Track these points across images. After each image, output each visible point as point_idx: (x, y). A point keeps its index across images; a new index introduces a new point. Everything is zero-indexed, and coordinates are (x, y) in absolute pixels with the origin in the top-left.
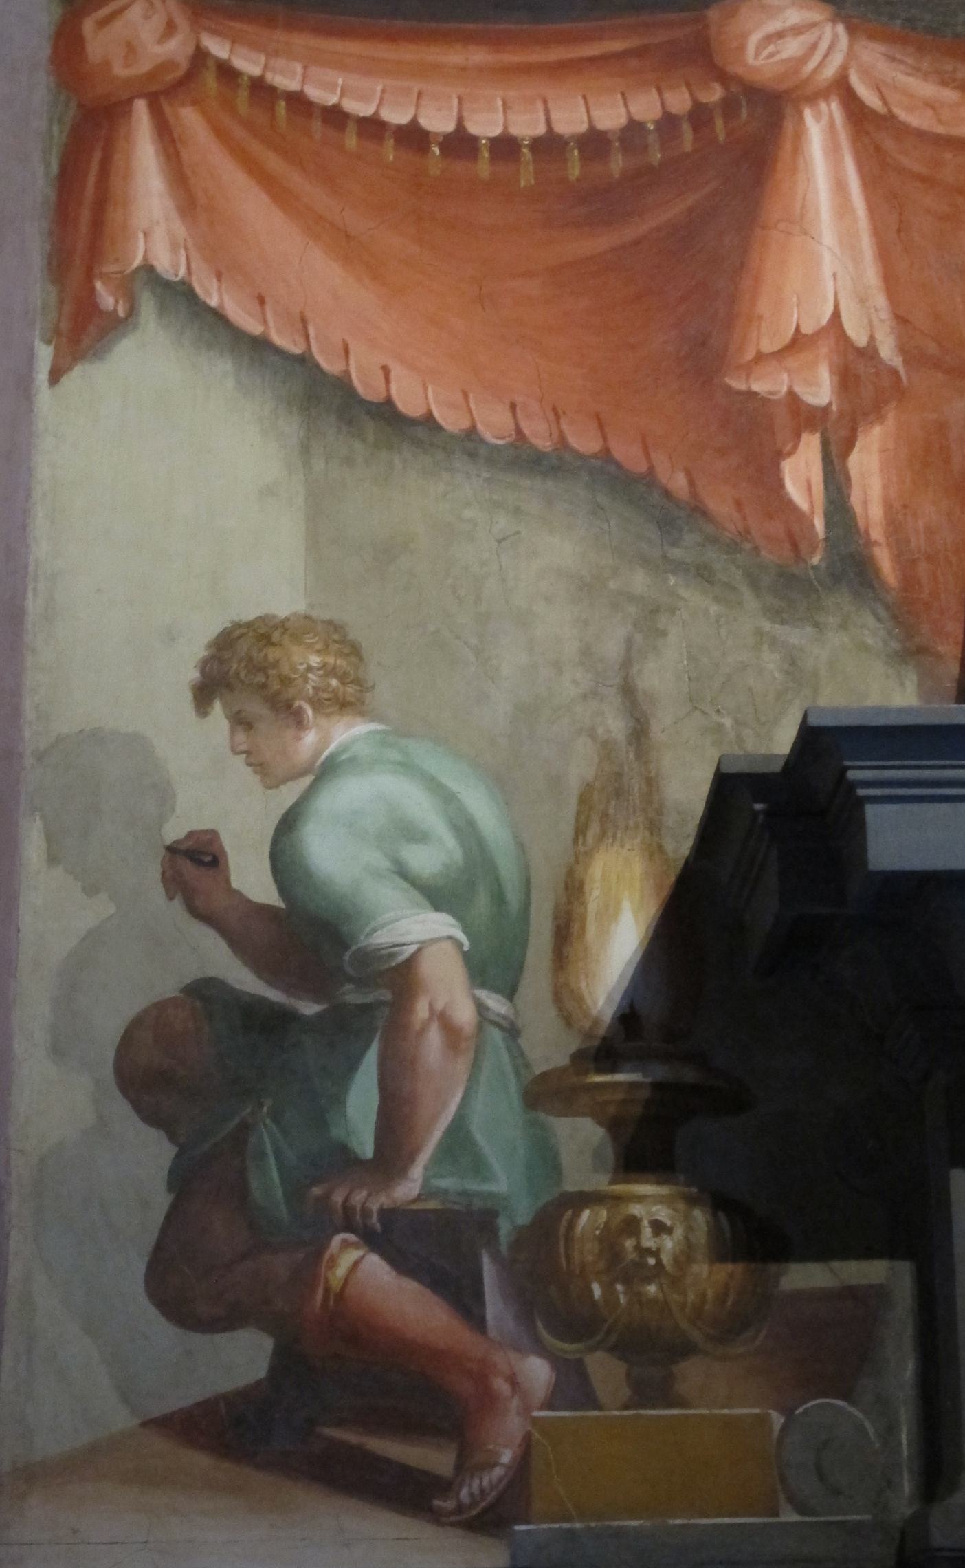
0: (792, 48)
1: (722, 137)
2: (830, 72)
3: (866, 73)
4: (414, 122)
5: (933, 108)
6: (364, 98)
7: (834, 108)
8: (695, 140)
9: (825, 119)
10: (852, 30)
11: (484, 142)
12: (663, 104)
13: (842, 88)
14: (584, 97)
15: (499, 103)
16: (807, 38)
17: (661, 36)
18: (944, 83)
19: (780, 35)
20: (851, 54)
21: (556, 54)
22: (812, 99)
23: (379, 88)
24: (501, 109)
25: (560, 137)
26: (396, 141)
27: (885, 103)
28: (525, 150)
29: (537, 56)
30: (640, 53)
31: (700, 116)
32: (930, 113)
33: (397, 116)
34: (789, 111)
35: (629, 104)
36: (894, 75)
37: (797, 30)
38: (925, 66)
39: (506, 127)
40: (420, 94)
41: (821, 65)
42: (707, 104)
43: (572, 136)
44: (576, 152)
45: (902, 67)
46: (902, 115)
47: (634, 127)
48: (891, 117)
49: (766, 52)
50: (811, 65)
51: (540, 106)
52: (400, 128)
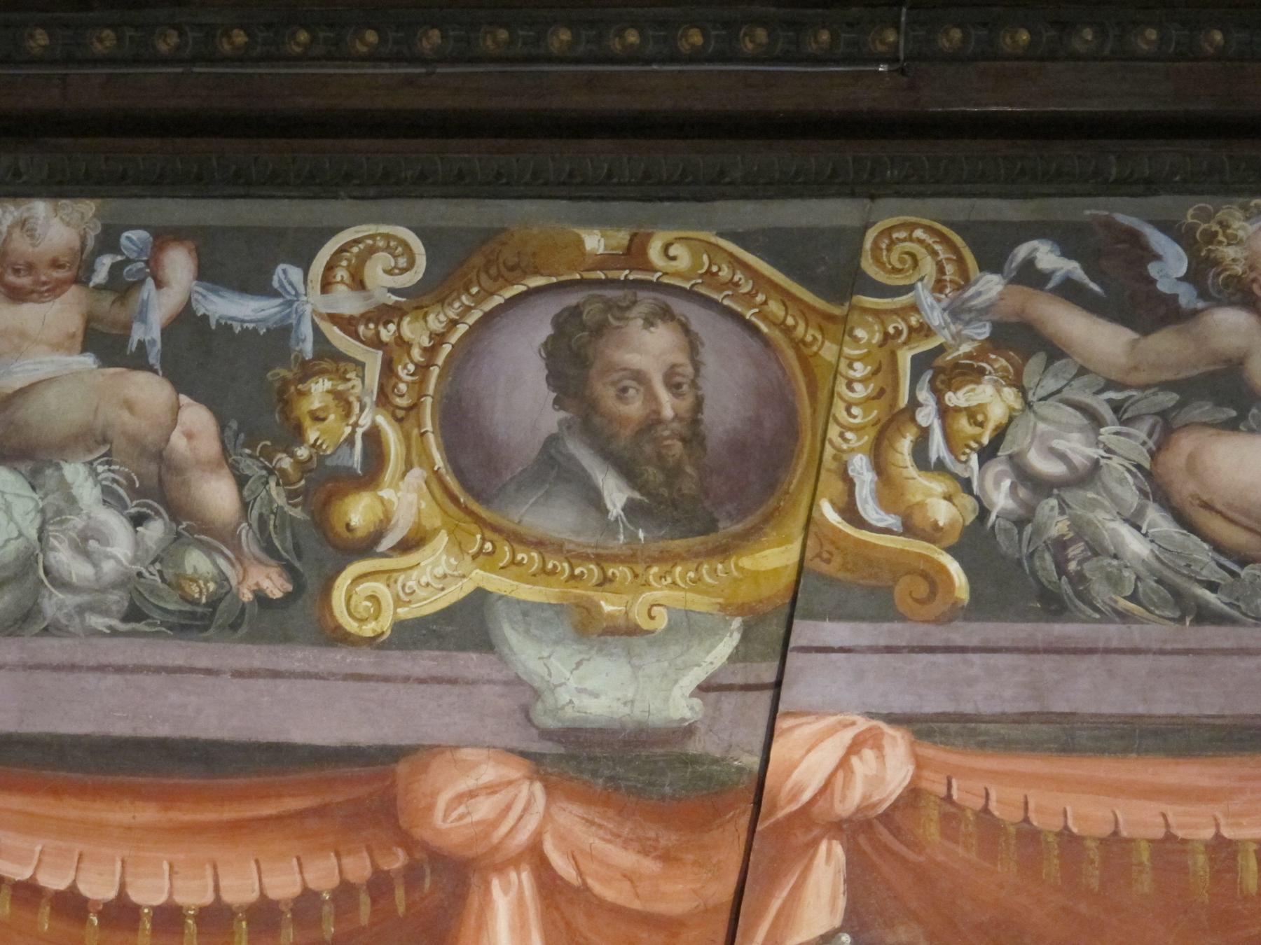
0: (484, 808)
1: (401, 909)
2: (523, 837)
3: (561, 838)
4: (73, 888)
5: (631, 880)
6: (20, 859)
7: (524, 879)
8: (374, 912)
9: (515, 888)
10: (549, 789)
11: (146, 911)
12: (341, 872)
13: (535, 856)
14: (257, 862)
15: (166, 867)
16: (500, 798)
17: (338, 796)
18: (645, 852)
19: (472, 794)
20: (547, 816)
21: (230, 813)
22: (500, 869)
23: (38, 848)
24: (167, 874)
25: (229, 908)
26: (52, 908)
27: (580, 873)
28: (190, 922)
29: (209, 815)
30: (320, 812)
31: (380, 885)
32: (626, 885)
33: (54, 881)
34: (475, 880)
35: (304, 870)
36: (591, 841)
37: (491, 789)
38: (625, 831)
39: (171, 894)
40: (81, 856)
41: (513, 829)
42: (388, 871)
43: (240, 907)
44: (244, 924)
45: (601, 832)
46: (597, 887)
47: (308, 896)
48: (586, 888)
49: (455, 815)
50: (504, 829)
51: (209, 872)
52: (58, 894)
